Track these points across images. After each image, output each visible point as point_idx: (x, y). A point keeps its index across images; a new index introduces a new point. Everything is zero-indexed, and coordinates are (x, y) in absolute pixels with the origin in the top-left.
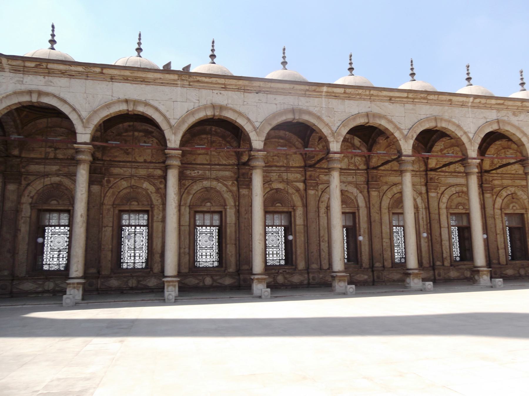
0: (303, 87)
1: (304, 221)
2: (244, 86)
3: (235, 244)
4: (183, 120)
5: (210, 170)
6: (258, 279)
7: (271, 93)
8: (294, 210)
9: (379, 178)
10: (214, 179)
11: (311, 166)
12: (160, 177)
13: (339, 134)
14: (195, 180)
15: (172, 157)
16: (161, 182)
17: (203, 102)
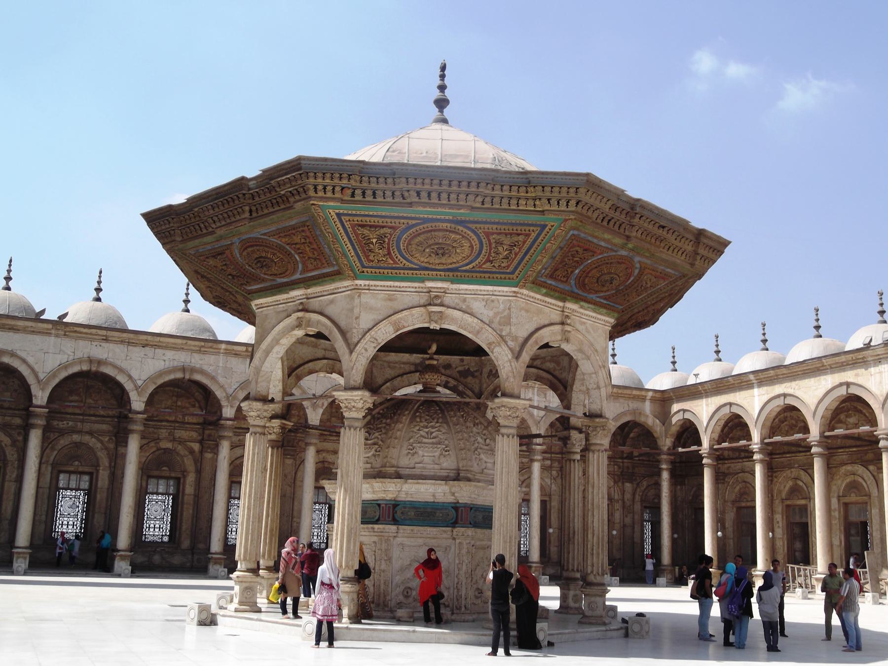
0: (197, 343)
1: (195, 490)
2: (129, 339)
3: (105, 514)
4: (54, 375)
5: (82, 421)
6: (121, 556)
7: (159, 347)
8: (185, 477)
9: (298, 443)
10: (87, 433)
11: (210, 424)
12: (18, 427)
13: (235, 398)
14: (62, 433)
15: (37, 416)
16: (19, 434)
17: (79, 355)
